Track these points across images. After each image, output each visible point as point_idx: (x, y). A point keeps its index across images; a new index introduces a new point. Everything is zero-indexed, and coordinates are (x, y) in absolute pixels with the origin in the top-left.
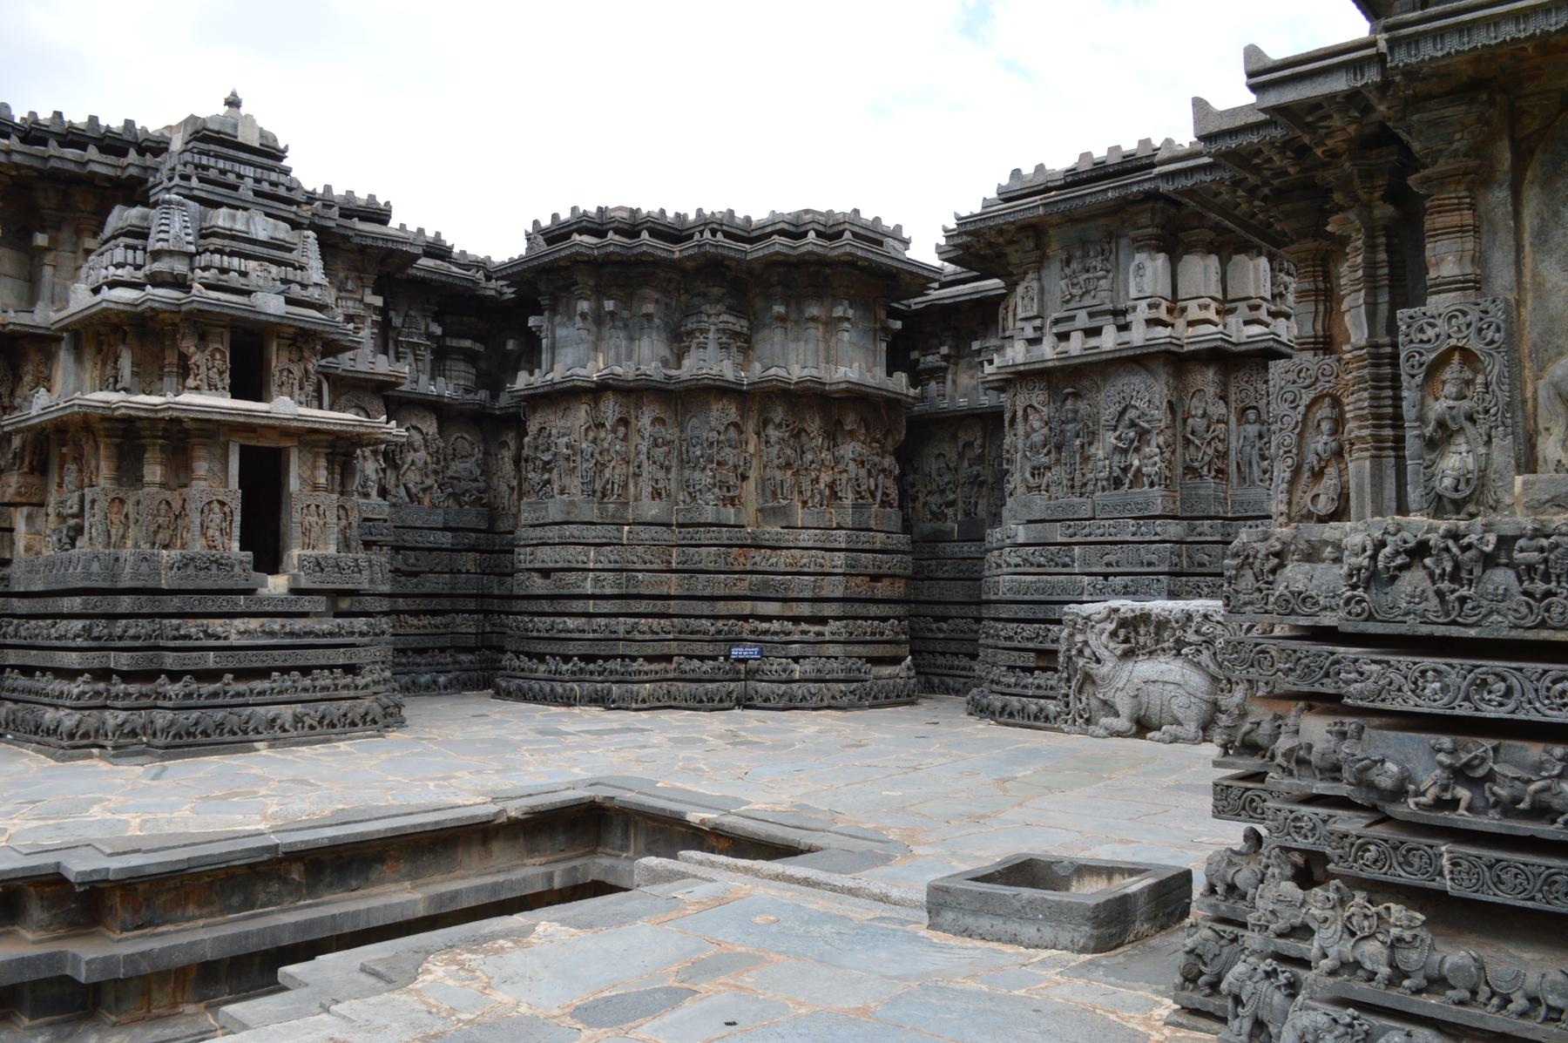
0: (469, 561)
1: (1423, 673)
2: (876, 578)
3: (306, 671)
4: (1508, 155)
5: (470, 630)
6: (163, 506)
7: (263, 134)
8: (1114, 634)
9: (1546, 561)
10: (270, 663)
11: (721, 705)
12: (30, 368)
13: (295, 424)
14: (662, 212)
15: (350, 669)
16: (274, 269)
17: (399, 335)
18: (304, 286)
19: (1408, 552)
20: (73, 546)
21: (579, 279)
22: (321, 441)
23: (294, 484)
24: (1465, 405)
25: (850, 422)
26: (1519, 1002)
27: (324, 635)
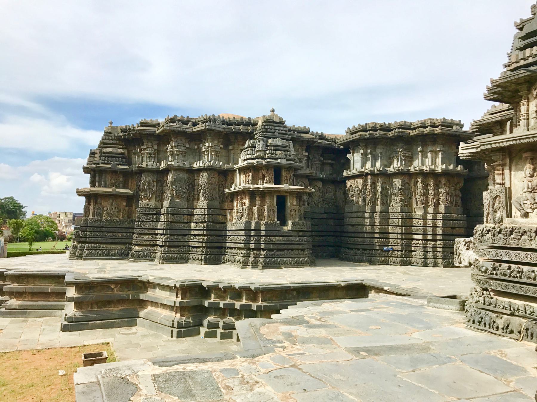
0: (331, 222)
1: (489, 252)
2: (453, 228)
3: (292, 250)
4: (508, 161)
5: (332, 241)
6: (260, 210)
7: (280, 119)
8: (465, 245)
9: (506, 233)
10: (285, 248)
11: (404, 265)
12: (229, 177)
13: (289, 190)
14: (385, 123)
15: (302, 250)
16: (283, 152)
17: (312, 161)
18: (290, 156)
19: (487, 231)
20: (241, 219)
21: (360, 144)
22: (295, 193)
23: (288, 204)
24: (500, 205)
25: (443, 181)
26: (502, 307)
27: (296, 241)
